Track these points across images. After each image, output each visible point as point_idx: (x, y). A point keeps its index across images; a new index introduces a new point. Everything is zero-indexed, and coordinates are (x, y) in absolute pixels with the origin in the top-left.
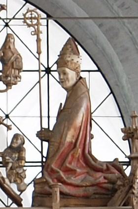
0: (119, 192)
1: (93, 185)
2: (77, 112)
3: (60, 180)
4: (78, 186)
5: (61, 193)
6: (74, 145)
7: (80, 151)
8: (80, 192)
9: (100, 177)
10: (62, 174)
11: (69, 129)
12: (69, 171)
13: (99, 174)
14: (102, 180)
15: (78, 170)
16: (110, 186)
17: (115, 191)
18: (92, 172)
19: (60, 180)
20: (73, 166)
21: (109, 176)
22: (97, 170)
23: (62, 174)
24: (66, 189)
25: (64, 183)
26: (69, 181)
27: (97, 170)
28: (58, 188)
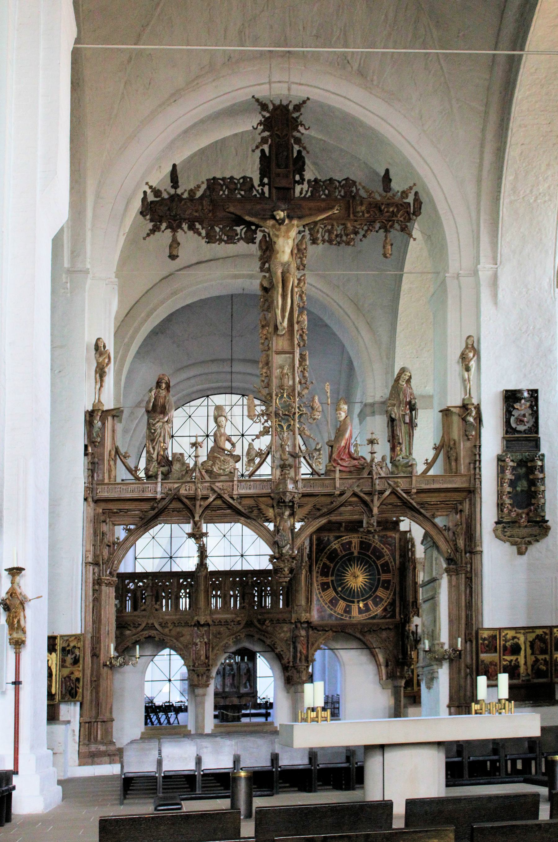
0: (365, 469)
1: (353, 466)
2: (346, 432)
3: (338, 464)
4: (346, 467)
5: (340, 470)
6: (345, 447)
7: (347, 450)
8: (347, 469)
9: (355, 462)
10: (339, 461)
11: (342, 440)
12: (342, 459)
13: (356, 461)
14: (357, 464)
15: (347, 459)
16: (360, 467)
17: (364, 468)
18: (352, 461)
19: (338, 464)
20: (344, 457)
21: (360, 462)
22: (355, 459)
23: (339, 461)
24: (342, 468)
25: (341, 466)
26: (342, 464)
27: (355, 459)
28: (338, 468)
